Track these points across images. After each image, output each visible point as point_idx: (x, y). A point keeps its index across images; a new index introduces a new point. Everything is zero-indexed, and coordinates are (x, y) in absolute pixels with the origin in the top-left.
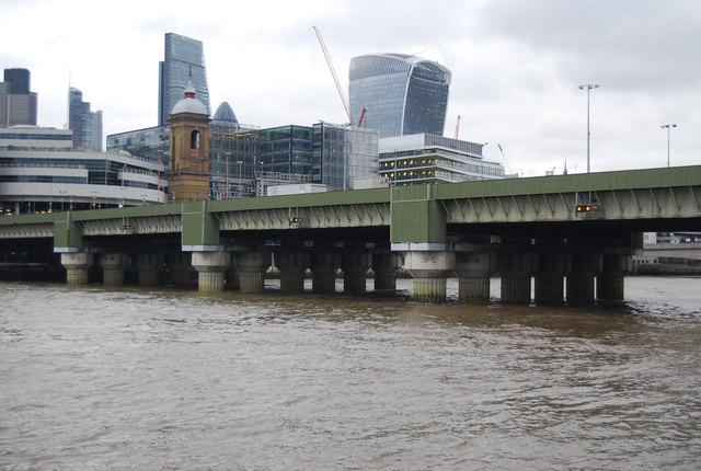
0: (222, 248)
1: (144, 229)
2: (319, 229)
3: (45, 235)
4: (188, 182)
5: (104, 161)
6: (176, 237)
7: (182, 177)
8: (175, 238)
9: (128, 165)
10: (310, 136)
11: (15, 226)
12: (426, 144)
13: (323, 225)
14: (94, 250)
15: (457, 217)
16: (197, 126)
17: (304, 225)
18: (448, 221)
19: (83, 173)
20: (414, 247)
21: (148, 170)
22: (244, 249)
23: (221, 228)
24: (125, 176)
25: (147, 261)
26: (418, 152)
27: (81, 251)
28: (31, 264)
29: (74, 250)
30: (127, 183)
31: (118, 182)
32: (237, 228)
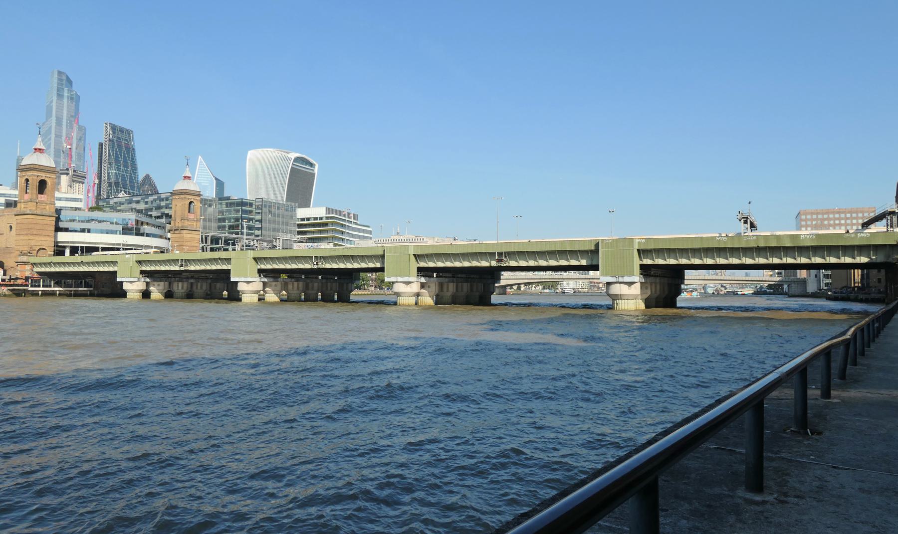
1: (192, 268)
4: (186, 235)
7: (182, 231)
8: (228, 272)
10: (254, 206)
11: (49, 264)
12: (326, 213)
14: (148, 280)
16: (192, 198)
19: (120, 228)
20: (400, 279)
26: (321, 218)
27: (139, 280)
28: (80, 289)
29: (135, 280)
30: (148, 235)
31: (139, 233)
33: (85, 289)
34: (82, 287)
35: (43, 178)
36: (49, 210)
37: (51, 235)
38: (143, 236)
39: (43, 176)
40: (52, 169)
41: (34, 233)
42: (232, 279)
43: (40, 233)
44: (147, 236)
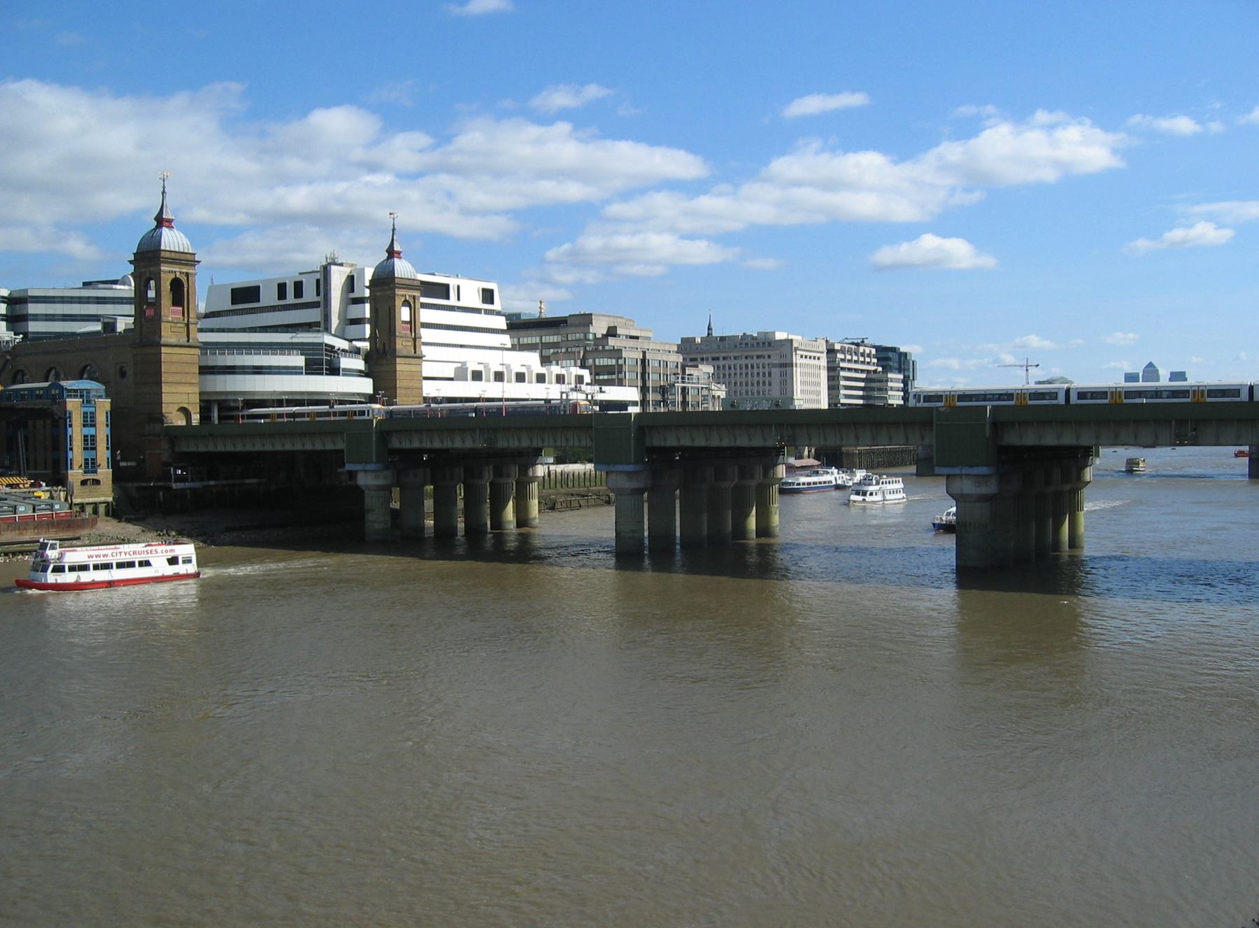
3: (329, 446)
5: (321, 344)
19: (299, 360)
28: (247, 481)
31: (334, 371)
33: (254, 481)
35: (178, 275)
37: (193, 381)
38: (339, 374)
40: (189, 257)
44: (343, 375)
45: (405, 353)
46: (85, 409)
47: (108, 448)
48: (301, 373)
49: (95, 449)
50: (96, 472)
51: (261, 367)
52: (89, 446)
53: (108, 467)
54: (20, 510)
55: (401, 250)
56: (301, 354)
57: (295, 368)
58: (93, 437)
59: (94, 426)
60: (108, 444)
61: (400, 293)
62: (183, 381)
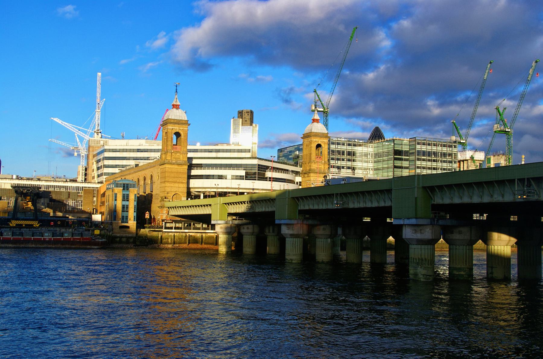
0: (300, 222)
2: (354, 209)
6: (273, 213)
9: (274, 168)
13: (357, 206)
15: (438, 200)
17: (346, 206)
18: (433, 202)
20: (407, 222)
21: (288, 170)
22: (316, 222)
23: (299, 208)
24: (269, 174)
25: (271, 231)
31: (263, 178)
32: (271, 210)
34: (209, 230)
36: (183, 158)
37: (184, 181)
39: (177, 128)
41: (170, 180)
42: (277, 222)
43: (175, 180)
45: (317, 171)
46: (124, 193)
47: (135, 212)
48: (243, 179)
49: (128, 211)
50: (127, 222)
51: (202, 176)
52: (125, 210)
53: (134, 221)
54: (46, 235)
55: (180, 104)
56: (244, 170)
57: (241, 176)
58: (127, 207)
59: (128, 201)
60: (135, 209)
61: (315, 140)
62: (178, 181)
